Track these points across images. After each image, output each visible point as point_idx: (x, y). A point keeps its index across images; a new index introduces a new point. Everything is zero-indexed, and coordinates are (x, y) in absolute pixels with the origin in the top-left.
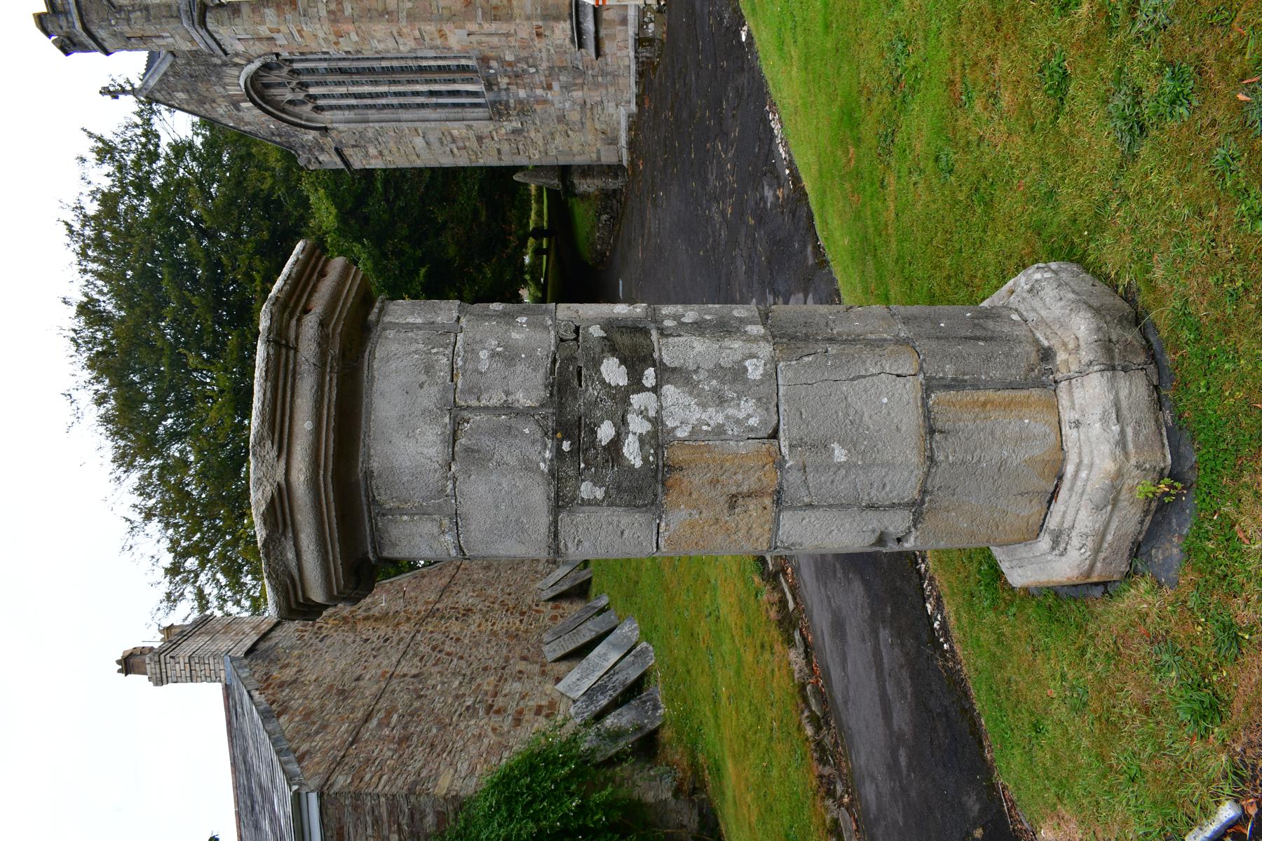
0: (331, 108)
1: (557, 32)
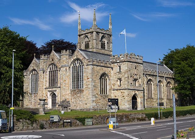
0: (32, 76)
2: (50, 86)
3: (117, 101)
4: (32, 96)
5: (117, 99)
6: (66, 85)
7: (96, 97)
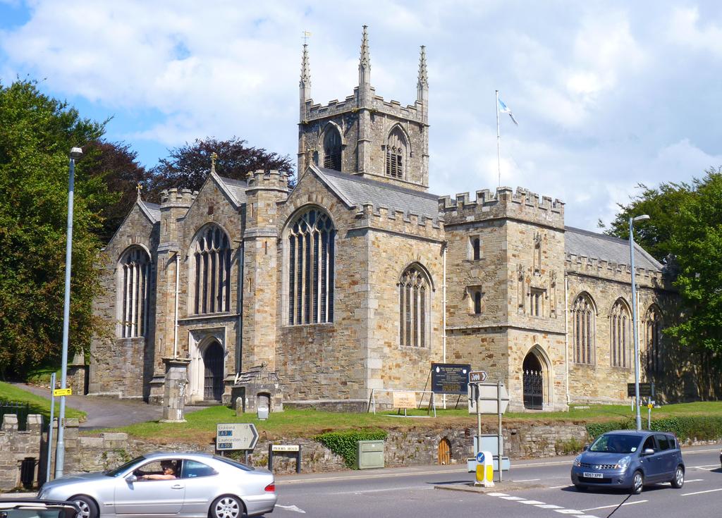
0: (126, 276)
2: (201, 309)
3: (465, 372)
4: (126, 351)
5: (468, 367)
6: (266, 309)
7: (384, 357)
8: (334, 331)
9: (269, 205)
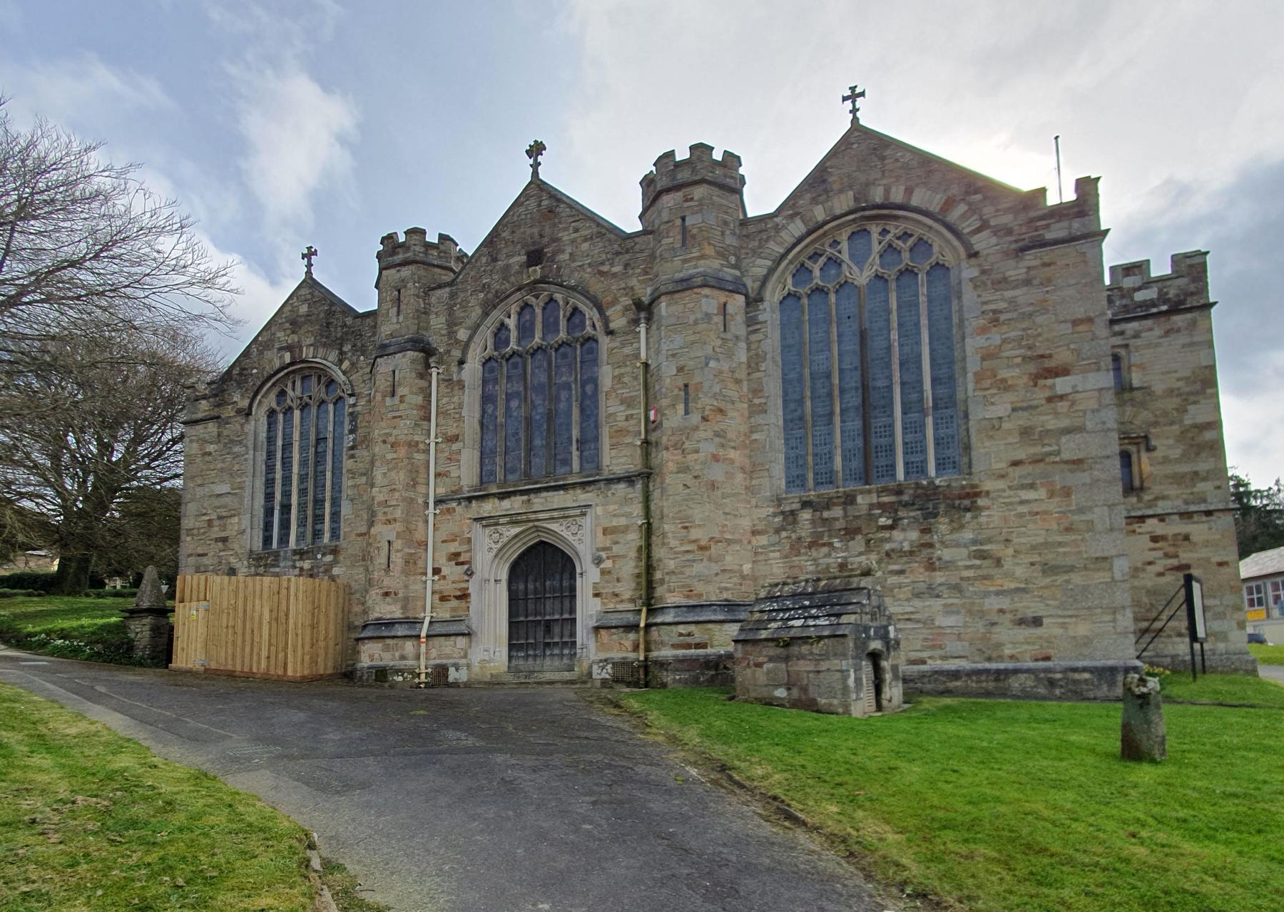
1: (393, 608)
6: (732, 454)
8: (978, 495)
9: (726, 223)
